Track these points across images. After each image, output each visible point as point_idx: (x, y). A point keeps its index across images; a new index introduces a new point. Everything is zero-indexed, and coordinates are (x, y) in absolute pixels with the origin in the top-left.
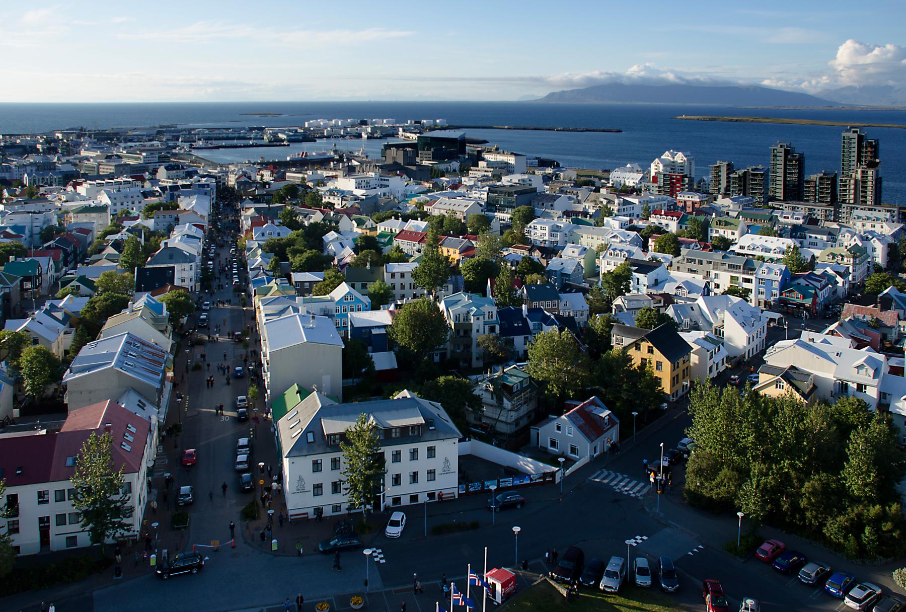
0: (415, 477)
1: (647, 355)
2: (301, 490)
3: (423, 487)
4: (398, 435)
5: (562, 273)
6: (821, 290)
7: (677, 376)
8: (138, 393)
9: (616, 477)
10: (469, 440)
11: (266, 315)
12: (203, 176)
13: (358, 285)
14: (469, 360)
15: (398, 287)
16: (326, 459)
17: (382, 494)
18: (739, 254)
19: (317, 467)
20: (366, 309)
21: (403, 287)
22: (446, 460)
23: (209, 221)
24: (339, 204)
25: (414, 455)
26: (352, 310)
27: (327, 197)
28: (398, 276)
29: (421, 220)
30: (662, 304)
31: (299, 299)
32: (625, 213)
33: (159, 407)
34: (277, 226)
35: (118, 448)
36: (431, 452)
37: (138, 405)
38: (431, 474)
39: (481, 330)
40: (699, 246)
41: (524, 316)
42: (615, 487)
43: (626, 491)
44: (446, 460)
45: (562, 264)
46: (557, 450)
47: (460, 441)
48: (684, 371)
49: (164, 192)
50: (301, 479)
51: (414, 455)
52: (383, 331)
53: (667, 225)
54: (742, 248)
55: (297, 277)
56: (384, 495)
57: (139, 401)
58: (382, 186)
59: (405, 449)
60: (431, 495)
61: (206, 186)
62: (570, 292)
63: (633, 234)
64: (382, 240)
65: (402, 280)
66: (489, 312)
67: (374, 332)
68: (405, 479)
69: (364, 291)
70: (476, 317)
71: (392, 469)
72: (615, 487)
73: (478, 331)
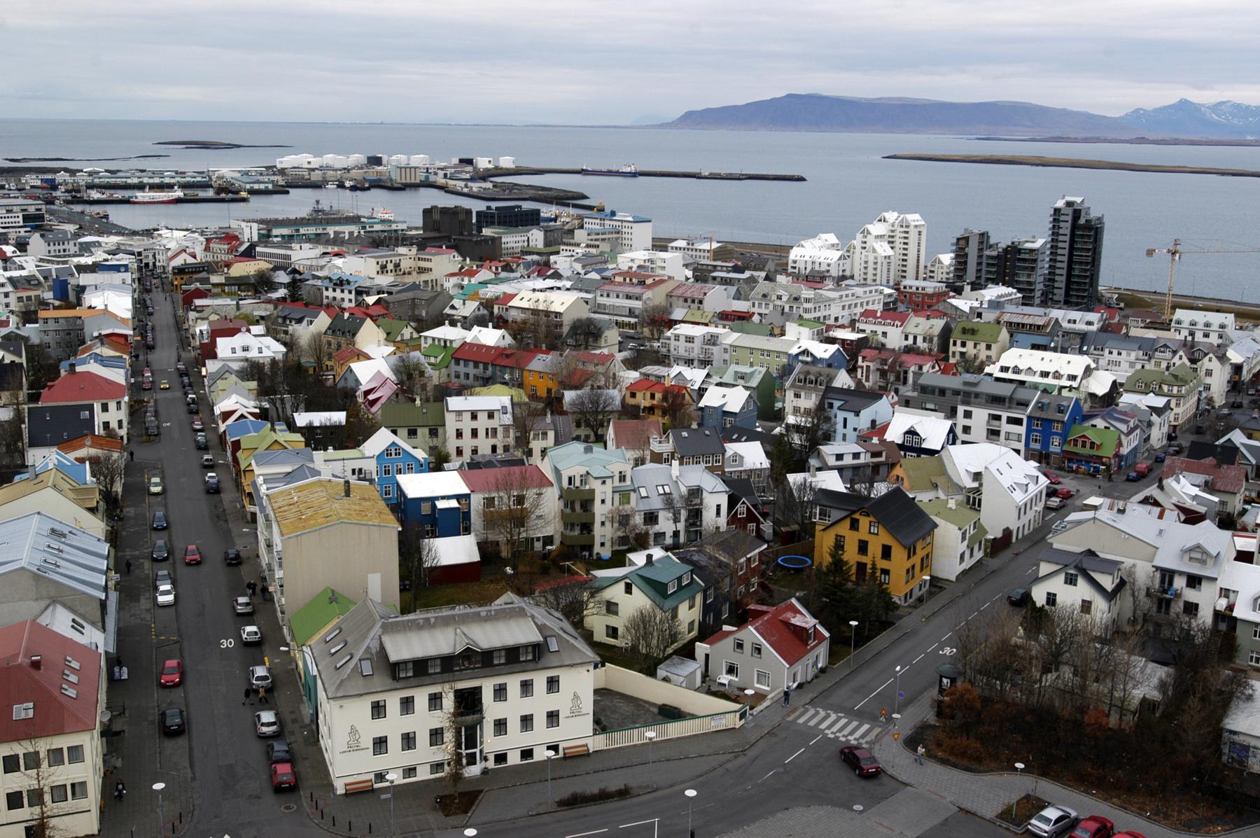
0: (527, 721)
1: (865, 537)
2: (354, 747)
3: (540, 736)
4: (503, 661)
5: (724, 412)
6: (1128, 434)
7: (913, 567)
8: (72, 609)
9: (828, 716)
10: (603, 665)
11: (265, 481)
12: (113, 253)
13: (403, 432)
14: (590, 547)
15: (467, 434)
16: (393, 702)
17: (477, 751)
18: (998, 379)
19: (378, 710)
20: (422, 468)
21: (474, 433)
22: (576, 696)
23: (134, 329)
24: (350, 301)
25: (526, 687)
26: (400, 472)
27: (330, 290)
28: (468, 416)
29: (494, 327)
30: (883, 459)
31: (319, 456)
32: (817, 314)
33: (104, 629)
34: (255, 336)
35: (56, 693)
36: (553, 684)
37: (73, 627)
38: (553, 717)
39: (608, 501)
40: (937, 368)
41: (675, 479)
42: (826, 731)
43: (844, 736)
44: (576, 696)
45: (724, 396)
46: (736, 679)
47: (596, 667)
48: (922, 559)
49: (46, 278)
50: (353, 731)
51: (526, 687)
52: (454, 504)
53: (885, 334)
54: (1004, 369)
55: (302, 419)
56: (481, 751)
57: (74, 621)
58: (422, 271)
59: (513, 683)
60: (554, 748)
61: (123, 269)
62: (738, 440)
63: (832, 348)
64: (432, 360)
65: (474, 424)
66: (620, 473)
67: (441, 505)
68: (514, 725)
69: (415, 441)
70: (600, 481)
71: (492, 709)
72: (826, 731)
73: (603, 501)
